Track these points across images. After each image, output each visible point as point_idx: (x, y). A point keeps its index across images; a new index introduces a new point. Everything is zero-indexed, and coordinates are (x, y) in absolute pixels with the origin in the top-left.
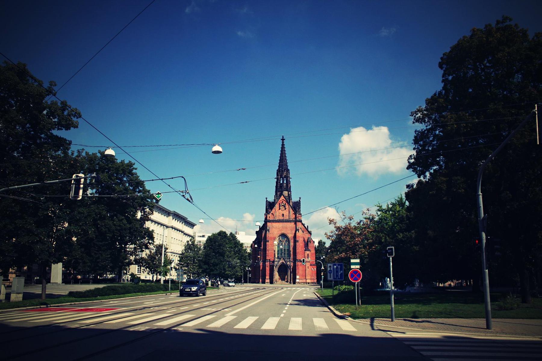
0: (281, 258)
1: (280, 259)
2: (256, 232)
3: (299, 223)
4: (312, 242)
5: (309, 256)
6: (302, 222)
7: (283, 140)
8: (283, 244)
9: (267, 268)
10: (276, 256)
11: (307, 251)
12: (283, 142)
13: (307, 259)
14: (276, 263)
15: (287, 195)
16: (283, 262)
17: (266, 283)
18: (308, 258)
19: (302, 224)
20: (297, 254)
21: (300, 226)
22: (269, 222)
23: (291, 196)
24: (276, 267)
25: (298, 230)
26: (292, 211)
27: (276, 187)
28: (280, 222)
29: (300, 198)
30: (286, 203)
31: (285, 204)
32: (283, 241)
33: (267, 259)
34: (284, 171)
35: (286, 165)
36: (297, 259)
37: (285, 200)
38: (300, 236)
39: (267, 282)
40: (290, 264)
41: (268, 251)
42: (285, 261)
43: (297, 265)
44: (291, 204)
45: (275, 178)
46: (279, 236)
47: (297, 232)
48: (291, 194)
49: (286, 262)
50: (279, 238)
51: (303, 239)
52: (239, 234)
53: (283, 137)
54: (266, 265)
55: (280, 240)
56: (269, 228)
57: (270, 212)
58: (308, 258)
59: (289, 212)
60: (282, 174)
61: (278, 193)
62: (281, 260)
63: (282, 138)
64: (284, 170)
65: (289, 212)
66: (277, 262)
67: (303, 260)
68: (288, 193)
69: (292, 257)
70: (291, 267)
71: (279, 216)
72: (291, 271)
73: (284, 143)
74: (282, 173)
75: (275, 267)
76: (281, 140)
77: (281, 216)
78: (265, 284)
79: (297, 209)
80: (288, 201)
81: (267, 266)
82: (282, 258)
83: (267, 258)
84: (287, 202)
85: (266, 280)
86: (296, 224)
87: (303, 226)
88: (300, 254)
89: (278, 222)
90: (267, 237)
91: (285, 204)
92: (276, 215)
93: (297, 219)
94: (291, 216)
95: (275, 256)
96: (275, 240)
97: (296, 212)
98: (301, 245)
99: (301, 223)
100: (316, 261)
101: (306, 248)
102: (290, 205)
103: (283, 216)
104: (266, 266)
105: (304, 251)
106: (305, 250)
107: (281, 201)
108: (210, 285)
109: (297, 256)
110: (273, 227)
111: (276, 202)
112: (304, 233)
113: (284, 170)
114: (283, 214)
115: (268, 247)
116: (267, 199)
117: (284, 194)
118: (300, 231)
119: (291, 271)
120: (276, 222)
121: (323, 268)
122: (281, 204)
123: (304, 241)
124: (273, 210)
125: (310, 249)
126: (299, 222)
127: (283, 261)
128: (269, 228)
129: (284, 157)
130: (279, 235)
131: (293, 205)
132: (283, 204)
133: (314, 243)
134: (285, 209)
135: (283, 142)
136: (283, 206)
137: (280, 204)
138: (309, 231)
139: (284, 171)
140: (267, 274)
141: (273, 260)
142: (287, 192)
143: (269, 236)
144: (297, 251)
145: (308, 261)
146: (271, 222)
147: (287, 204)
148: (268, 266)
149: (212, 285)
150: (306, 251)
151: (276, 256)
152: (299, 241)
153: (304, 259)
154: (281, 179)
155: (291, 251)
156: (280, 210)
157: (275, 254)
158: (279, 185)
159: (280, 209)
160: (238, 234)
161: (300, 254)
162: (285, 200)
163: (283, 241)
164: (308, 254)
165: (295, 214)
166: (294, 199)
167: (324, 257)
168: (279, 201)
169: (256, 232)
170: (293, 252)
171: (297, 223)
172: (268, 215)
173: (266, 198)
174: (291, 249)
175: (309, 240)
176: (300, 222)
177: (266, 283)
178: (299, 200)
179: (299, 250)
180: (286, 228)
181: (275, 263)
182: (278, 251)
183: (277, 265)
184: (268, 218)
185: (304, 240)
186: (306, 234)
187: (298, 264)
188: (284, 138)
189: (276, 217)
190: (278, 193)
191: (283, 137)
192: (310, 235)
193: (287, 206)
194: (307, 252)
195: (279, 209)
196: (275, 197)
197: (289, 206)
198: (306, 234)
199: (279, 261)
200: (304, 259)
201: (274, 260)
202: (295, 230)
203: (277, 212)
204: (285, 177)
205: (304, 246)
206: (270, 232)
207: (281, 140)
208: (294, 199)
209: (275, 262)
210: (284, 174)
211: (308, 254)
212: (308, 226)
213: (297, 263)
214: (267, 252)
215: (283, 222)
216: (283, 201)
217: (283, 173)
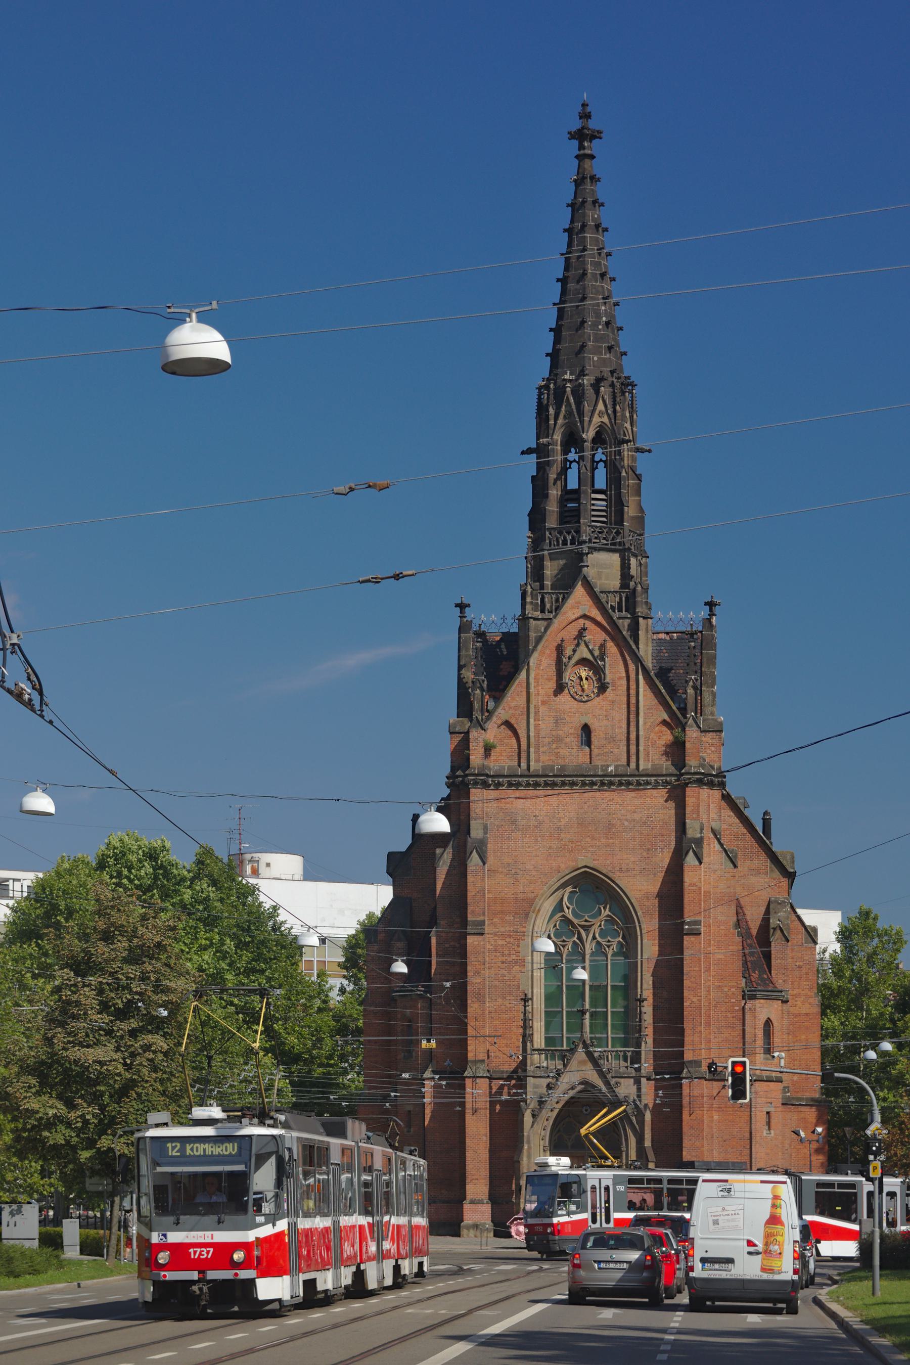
0: (572, 1051)
1: (565, 1057)
2: (391, 856)
3: (705, 792)
4: (798, 937)
5: (777, 1040)
6: (722, 785)
8: (589, 947)
9: (469, 1119)
10: (539, 1041)
11: (758, 1003)
13: (760, 1057)
14: (535, 1087)
15: (614, 583)
16: (585, 1082)
17: (468, 1228)
18: (768, 1051)
19: (727, 798)
20: (687, 1026)
21: (713, 815)
22: (486, 785)
23: (646, 590)
24: (534, 1116)
25: (699, 842)
26: (650, 694)
27: (536, 517)
28: (564, 784)
30: (610, 645)
31: (602, 647)
32: (587, 928)
33: (471, 1056)
34: (590, 392)
35: (610, 348)
36: (688, 1056)
37: (599, 618)
38: (708, 894)
39: (476, 1226)
40: (639, 1096)
41: (481, 999)
42: (602, 1075)
43: (685, 1101)
44: (646, 650)
45: (529, 451)
46: (564, 886)
47: (690, 859)
48: (644, 573)
49: (607, 1083)
50: (559, 907)
51: (733, 910)
52: (262, 869)
53: (585, 116)
54: (463, 1105)
55: (566, 921)
56: (486, 829)
57: (491, 713)
58: (768, 1051)
59: (632, 711)
60: (581, 413)
61: (550, 569)
62: (573, 1064)
63: (576, 124)
64: (596, 386)
65: (632, 711)
66: (545, 1082)
67: (734, 1064)
68: (625, 567)
69: (647, 1047)
70: (648, 1116)
71: (558, 740)
72: (648, 1143)
74: (579, 403)
75: (528, 1118)
76: (572, 136)
78: (458, 1235)
79: (690, 691)
80: (627, 622)
81: (475, 1111)
82: (581, 1053)
83: (475, 1050)
84: (613, 639)
85: (467, 1207)
86: (678, 796)
87: (729, 815)
88: (708, 1025)
89: (553, 785)
90: (470, 895)
91: (602, 647)
92: (538, 735)
93: (692, 763)
94: (647, 738)
95: (527, 1037)
96: (527, 915)
97: (684, 710)
98: (719, 955)
99: (716, 794)
100: (826, 1077)
101: (755, 975)
102: (638, 660)
103: (589, 743)
104: (468, 1106)
105: (736, 1001)
106: (749, 995)
107: (573, 630)
108: (72, 1251)
109: (687, 1039)
110: (514, 822)
111: (532, 635)
112: (744, 865)
113: (596, 386)
114: (586, 730)
115: (478, 973)
116: (470, 614)
117: (590, 572)
118: (712, 851)
119: (648, 1143)
120: (536, 785)
121: (875, 1128)
122: (568, 651)
123: (738, 924)
124: (514, 697)
125: (780, 984)
126: (700, 782)
127: (593, 1077)
128: (486, 829)
129: (589, 282)
130: (554, 882)
131: (657, 655)
132: (583, 652)
133: (815, 943)
134: (603, 688)
136: (583, 662)
138: (774, 858)
139: (590, 392)
140: (470, 1166)
141: (509, 1067)
142: (615, 558)
143: (481, 893)
144: (690, 999)
145: (765, 1074)
146: (498, 785)
147: (612, 648)
148: (479, 1105)
149: (90, 1248)
150: (753, 997)
151: (539, 1041)
152: (703, 930)
153: (743, 1064)
154: (572, 456)
155: (641, 1000)
156: (564, 698)
157: (526, 1024)
158: (552, 507)
159: (560, 688)
160: (248, 869)
161: (708, 1025)
162: (599, 618)
163: (587, 928)
164: (768, 1022)
165: (676, 722)
167: (887, 1046)
168: (557, 624)
169: (391, 856)
170: (655, 1008)
171: (689, 791)
172: (473, 734)
173: (462, 606)
174: (646, 987)
175: (774, 922)
176: (711, 785)
177: (468, 1228)
178: (708, 622)
179: (703, 993)
180: (610, 829)
181: (529, 1089)
182: (552, 998)
183: (541, 1103)
184: (476, 758)
185: (740, 923)
186: (753, 879)
187: (696, 1092)
188: (593, 124)
189: (537, 746)
190: (550, 569)
191: (585, 116)
192: (785, 882)
193: (614, 668)
194: (764, 1009)
195: (552, 685)
196: (524, 595)
197: (632, 667)
198: (757, 872)
199: (559, 1074)
200: (743, 1064)
201: (523, 1064)
202: (673, 846)
203: (543, 709)
204: (599, 439)
205: (738, 965)
206: (491, 860)
209: (530, 1081)
210: (596, 419)
211: (768, 1022)
212: (766, 823)
213: (686, 1091)
214: (473, 1007)
215: (584, 784)
216: (584, 629)
217: (587, 408)
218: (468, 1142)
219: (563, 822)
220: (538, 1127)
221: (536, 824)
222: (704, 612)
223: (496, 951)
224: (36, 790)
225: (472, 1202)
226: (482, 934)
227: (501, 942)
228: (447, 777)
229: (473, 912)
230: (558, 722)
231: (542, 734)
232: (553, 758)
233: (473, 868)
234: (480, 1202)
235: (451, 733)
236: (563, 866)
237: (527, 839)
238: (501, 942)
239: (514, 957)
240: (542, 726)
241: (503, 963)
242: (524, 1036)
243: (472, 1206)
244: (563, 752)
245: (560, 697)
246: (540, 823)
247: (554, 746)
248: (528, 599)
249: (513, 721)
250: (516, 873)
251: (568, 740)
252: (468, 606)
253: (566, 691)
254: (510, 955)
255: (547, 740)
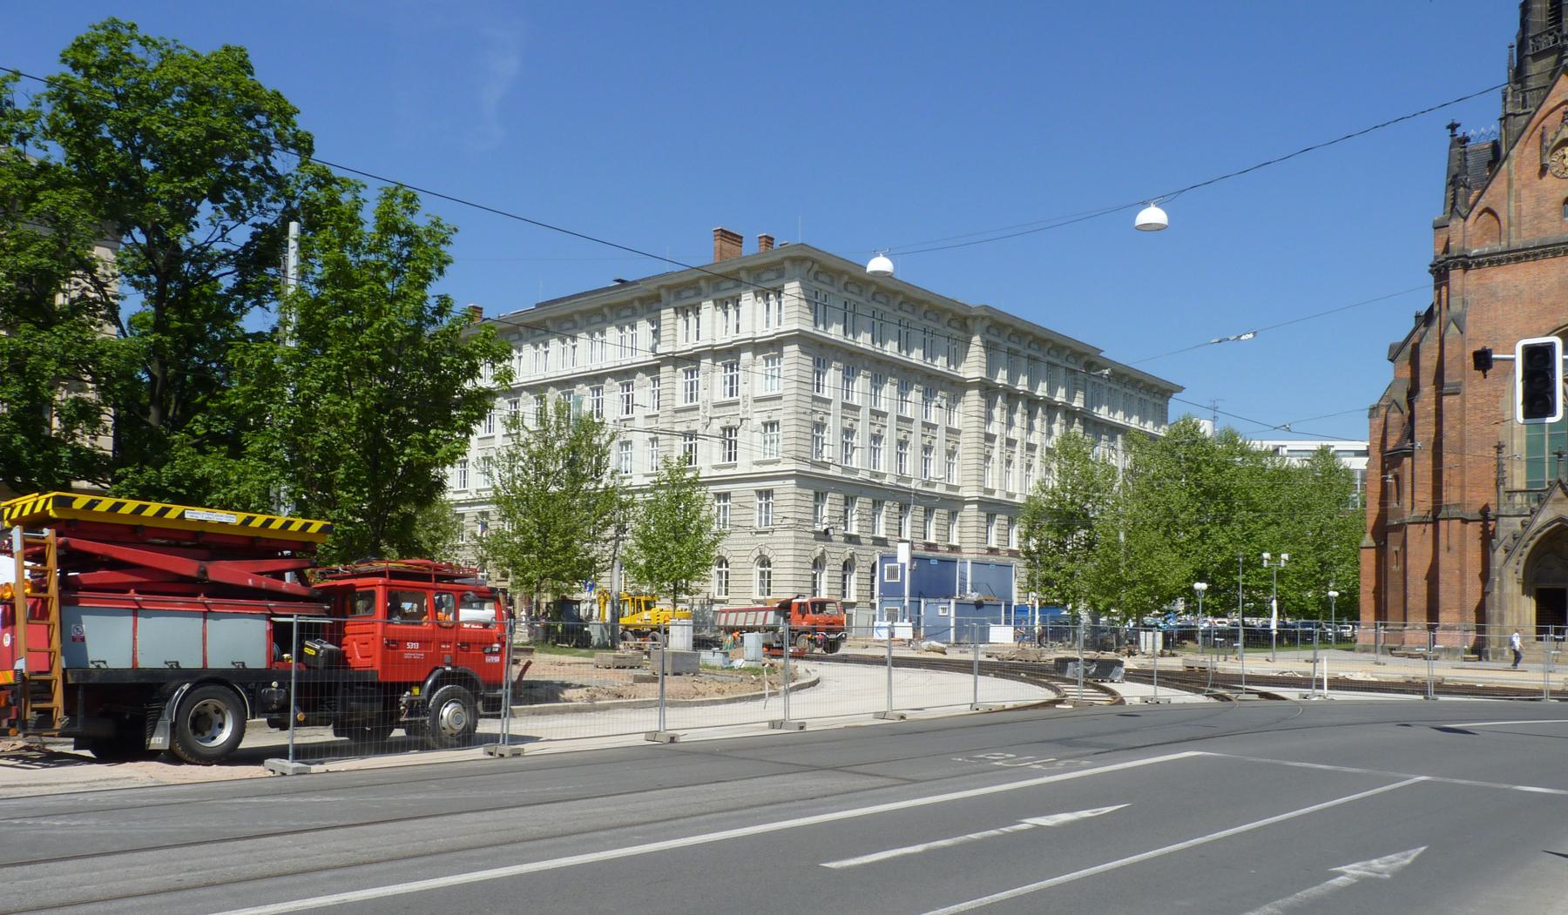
56: (1464, 303)
110: (1493, 294)
122: (1550, 135)
128: (1464, 303)
137: (1542, 136)
146: (1479, 265)
156: (1548, 178)
159: (1543, 170)
203: (1525, 193)
218: (1441, 575)
219: (1544, 288)
220: (1512, 563)
221: (1516, 293)
223: (1475, 409)
224: (878, 256)
225: (1445, 628)
226: (1458, 394)
227: (1480, 401)
228: (1431, 266)
229: (1449, 375)
230: (1538, 201)
231: (1524, 213)
232: (1535, 233)
233: (1450, 337)
234: (1452, 629)
235: (1435, 228)
236: (1544, 327)
237: (1506, 308)
238: (1480, 401)
239: (1494, 413)
240: (1524, 207)
241: (1482, 418)
242: (1497, 480)
243: (1446, 633)
244: (1545, 225)
245: (1544, 178)
246: (1521, 292)
247: (1536, 222)
248: (1509, 99)
249: (1493, 207)
250: (1496, 339)
251: (1549, 215)
252: (1458, 125)
253: (1549, 171)
254: (1489, 411)
255: (1528, 219)
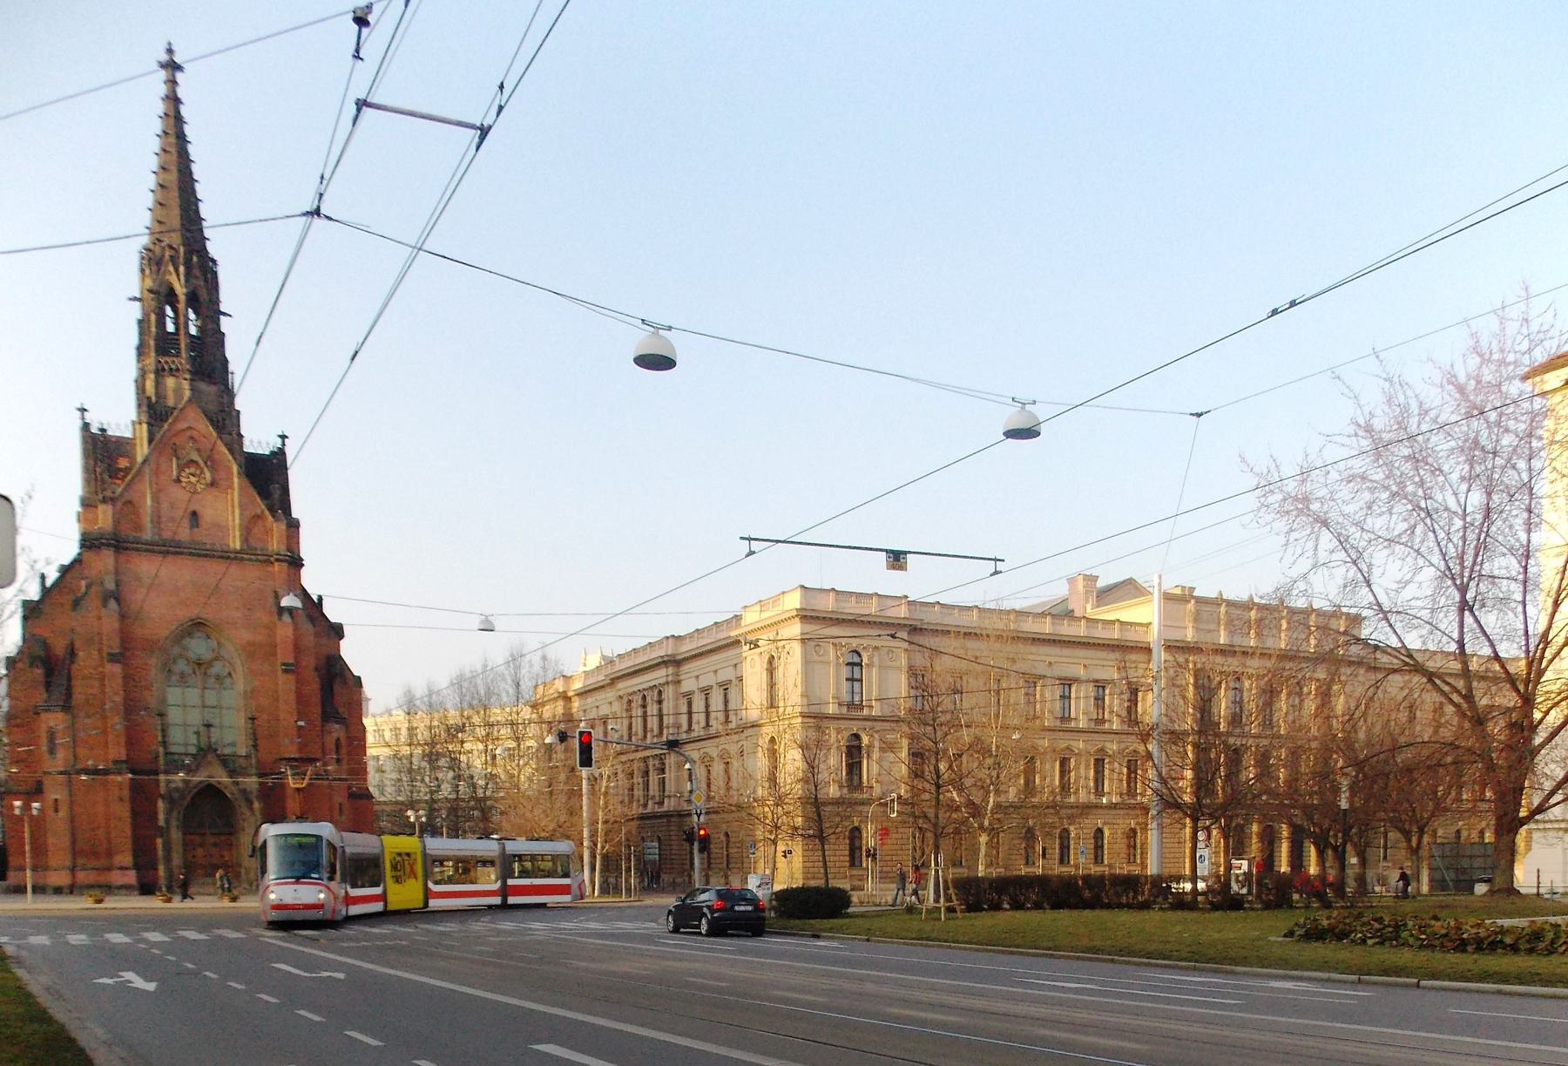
7: (172, 67)
12: (172, 82)
29: (283, 437)
53: (170, 51)
63: (164, 57)
73: (181, 93)
76: (163, 66)
77: (186, 523)
135: (172, 82)
166: (257, 438)
188: (177, 59)
191: (170, 51)
207: (163, 66)
208: (257, 438)
222: (279, 441)
